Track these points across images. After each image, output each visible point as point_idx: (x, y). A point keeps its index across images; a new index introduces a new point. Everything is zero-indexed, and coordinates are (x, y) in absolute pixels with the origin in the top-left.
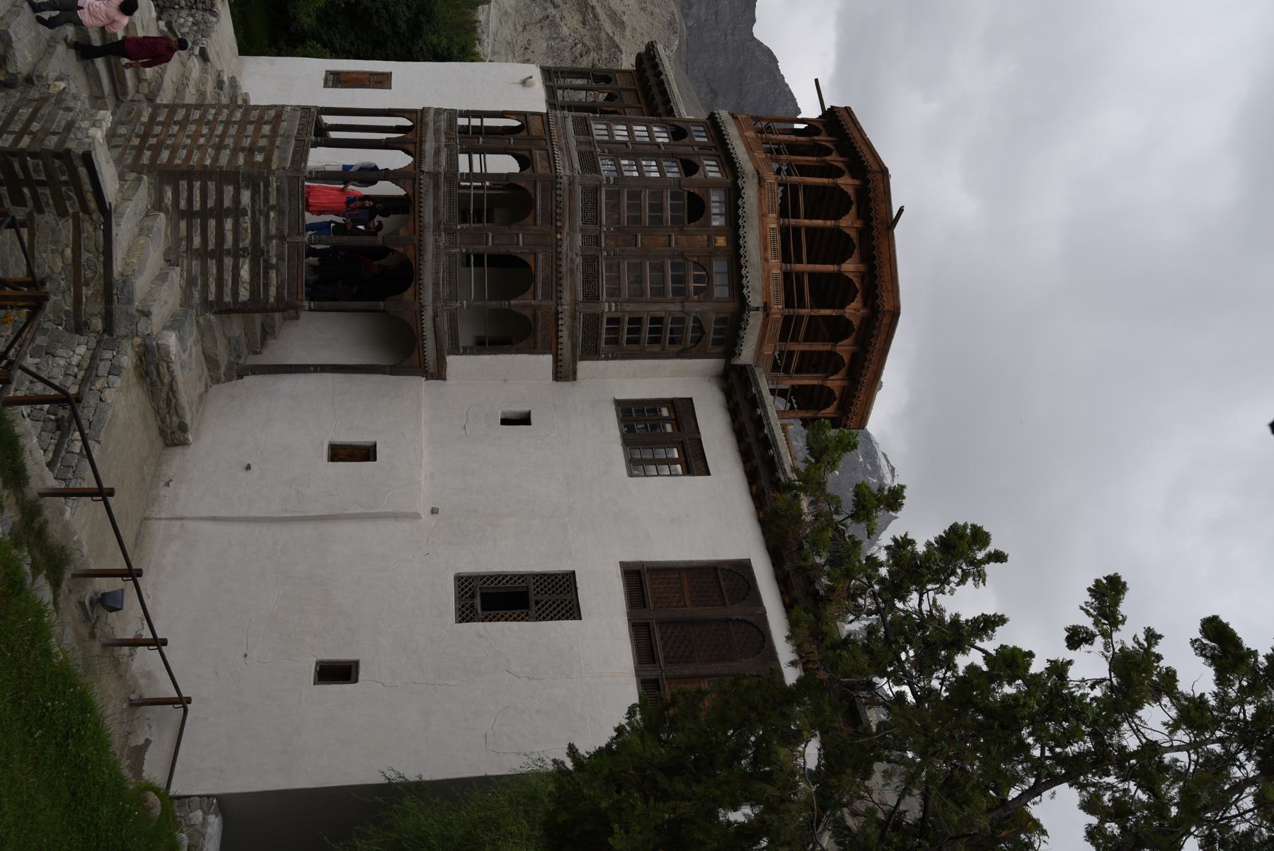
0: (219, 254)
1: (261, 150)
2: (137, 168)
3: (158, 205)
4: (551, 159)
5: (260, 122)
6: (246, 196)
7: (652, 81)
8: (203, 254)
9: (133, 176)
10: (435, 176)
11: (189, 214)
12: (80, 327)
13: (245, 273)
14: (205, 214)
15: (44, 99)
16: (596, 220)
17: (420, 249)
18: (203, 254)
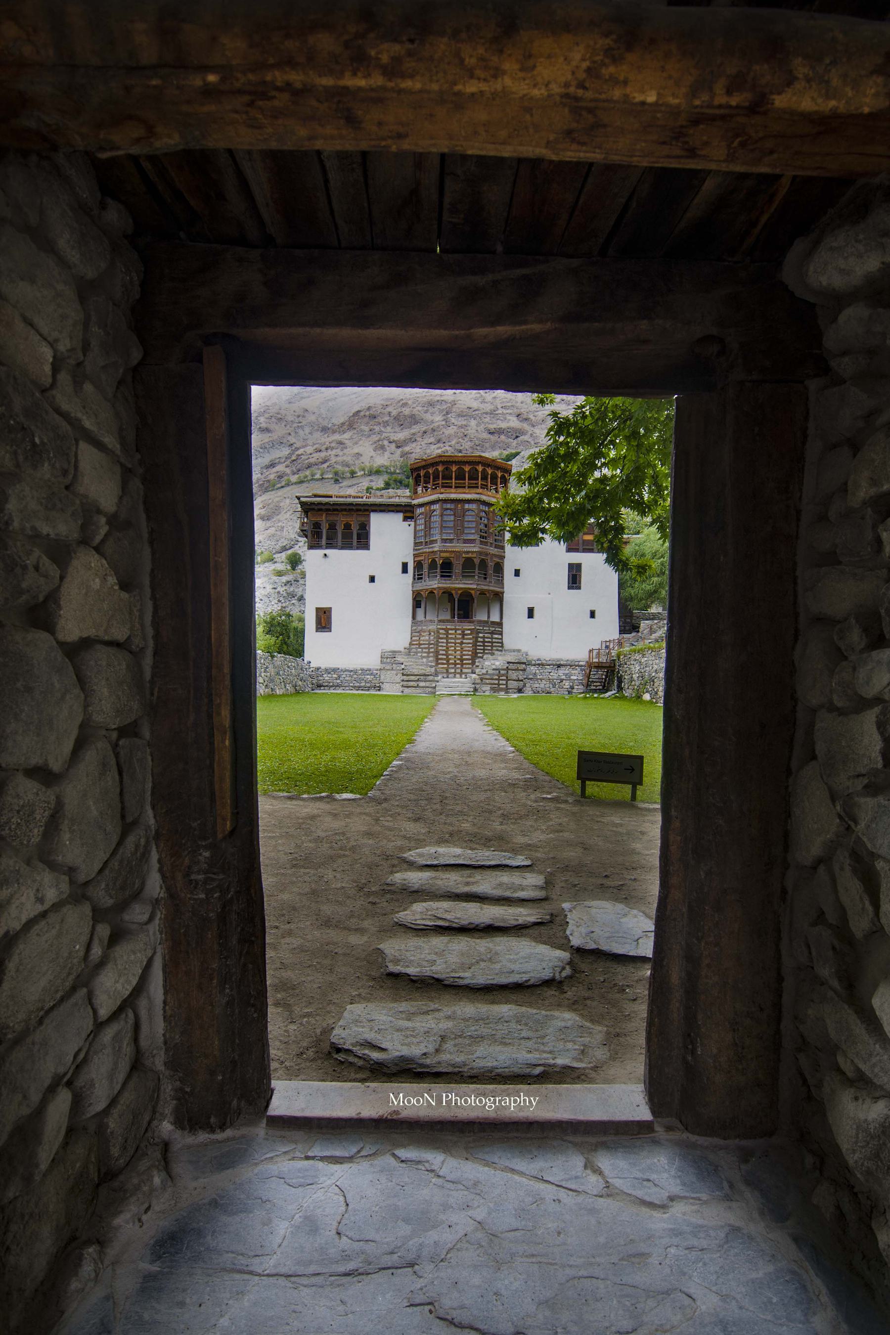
0: (492, 643)
1: (463, 632)
2: (473, 663)
3: (482, 657)
4: (468, 552)
5: (447, 634)
6: (481, 635)
7: (331, 508)
8: (492, 646)
9: (477, 664)
10: (478, 585)
11: (484, 650)
12: (524, 670)
13: (496, 636)
14: (484, 646)
15: (482, 679)
16: (487, 543)
17: (492, 591)
18: (492, 646)
